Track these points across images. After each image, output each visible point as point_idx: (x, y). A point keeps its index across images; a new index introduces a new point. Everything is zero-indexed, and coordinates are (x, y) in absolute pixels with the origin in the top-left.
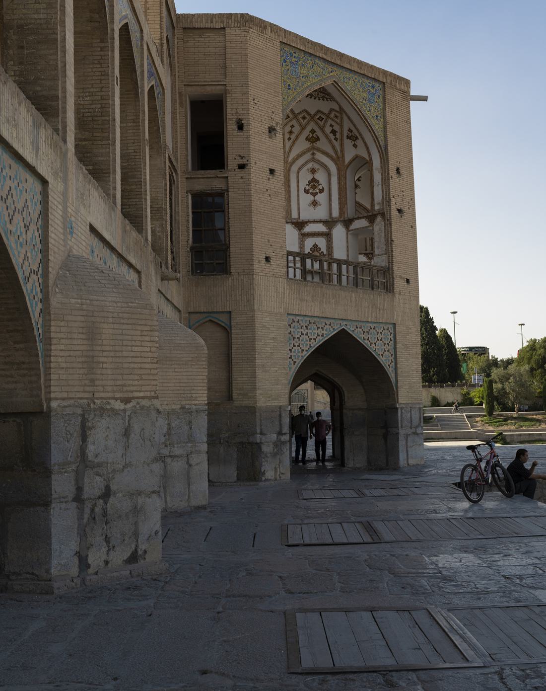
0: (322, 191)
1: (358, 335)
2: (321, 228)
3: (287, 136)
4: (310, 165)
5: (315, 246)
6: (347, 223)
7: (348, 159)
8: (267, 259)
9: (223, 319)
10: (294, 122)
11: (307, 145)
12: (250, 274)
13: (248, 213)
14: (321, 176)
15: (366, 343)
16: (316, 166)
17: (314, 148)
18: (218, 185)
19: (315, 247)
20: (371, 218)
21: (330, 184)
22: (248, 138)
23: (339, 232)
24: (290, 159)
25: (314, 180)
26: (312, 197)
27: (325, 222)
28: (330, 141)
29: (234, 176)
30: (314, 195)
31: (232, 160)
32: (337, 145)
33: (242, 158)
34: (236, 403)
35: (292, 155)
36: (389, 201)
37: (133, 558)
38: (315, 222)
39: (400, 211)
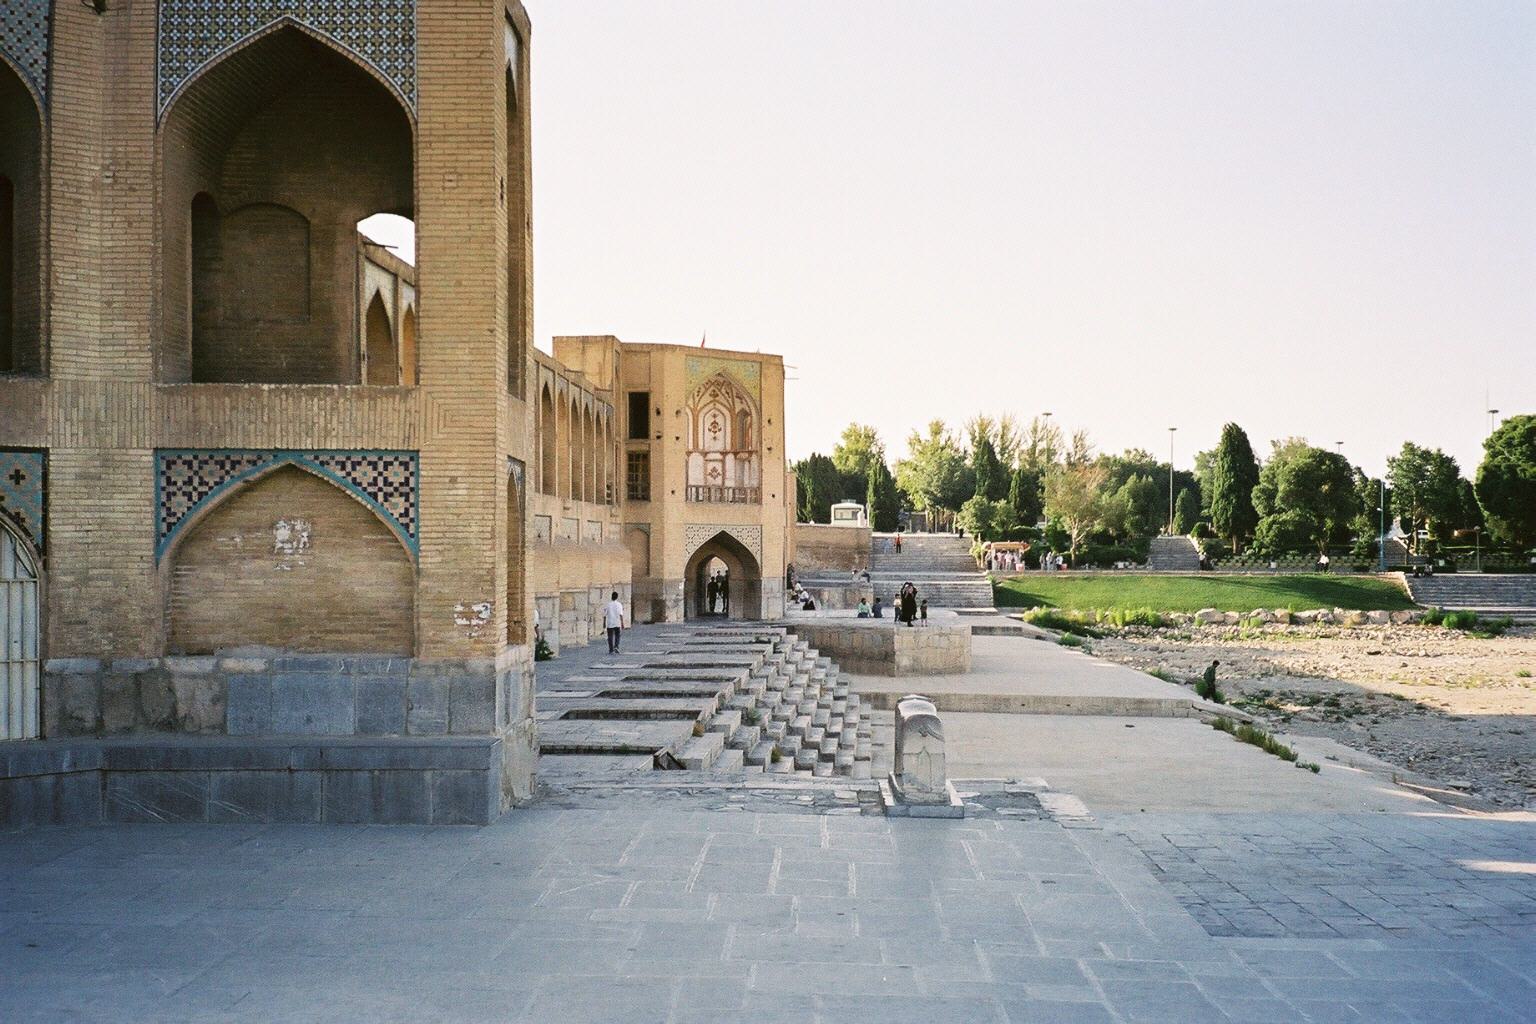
0: (720, 430)
1: (734, 534)
2: (719, 456)
6: (736, 454)
7: (737, 410)
8: (673, 492)
12: (661, 500)
13: (661, 465)
14: (719, 420)
15: (739, 539)
16: (717, 413)
17: (715, 400)
18: (644, 448)
19: (714, 470)
21: (725, 426)
22: (662, 420)
26: (712, 434)
27: (722, 453)
28: (725, 398)
29: (654, 442)
31: (653, 434)
34: (652, 576)
35: (700, 405)
36: (761, 443)
39: (769, 449)
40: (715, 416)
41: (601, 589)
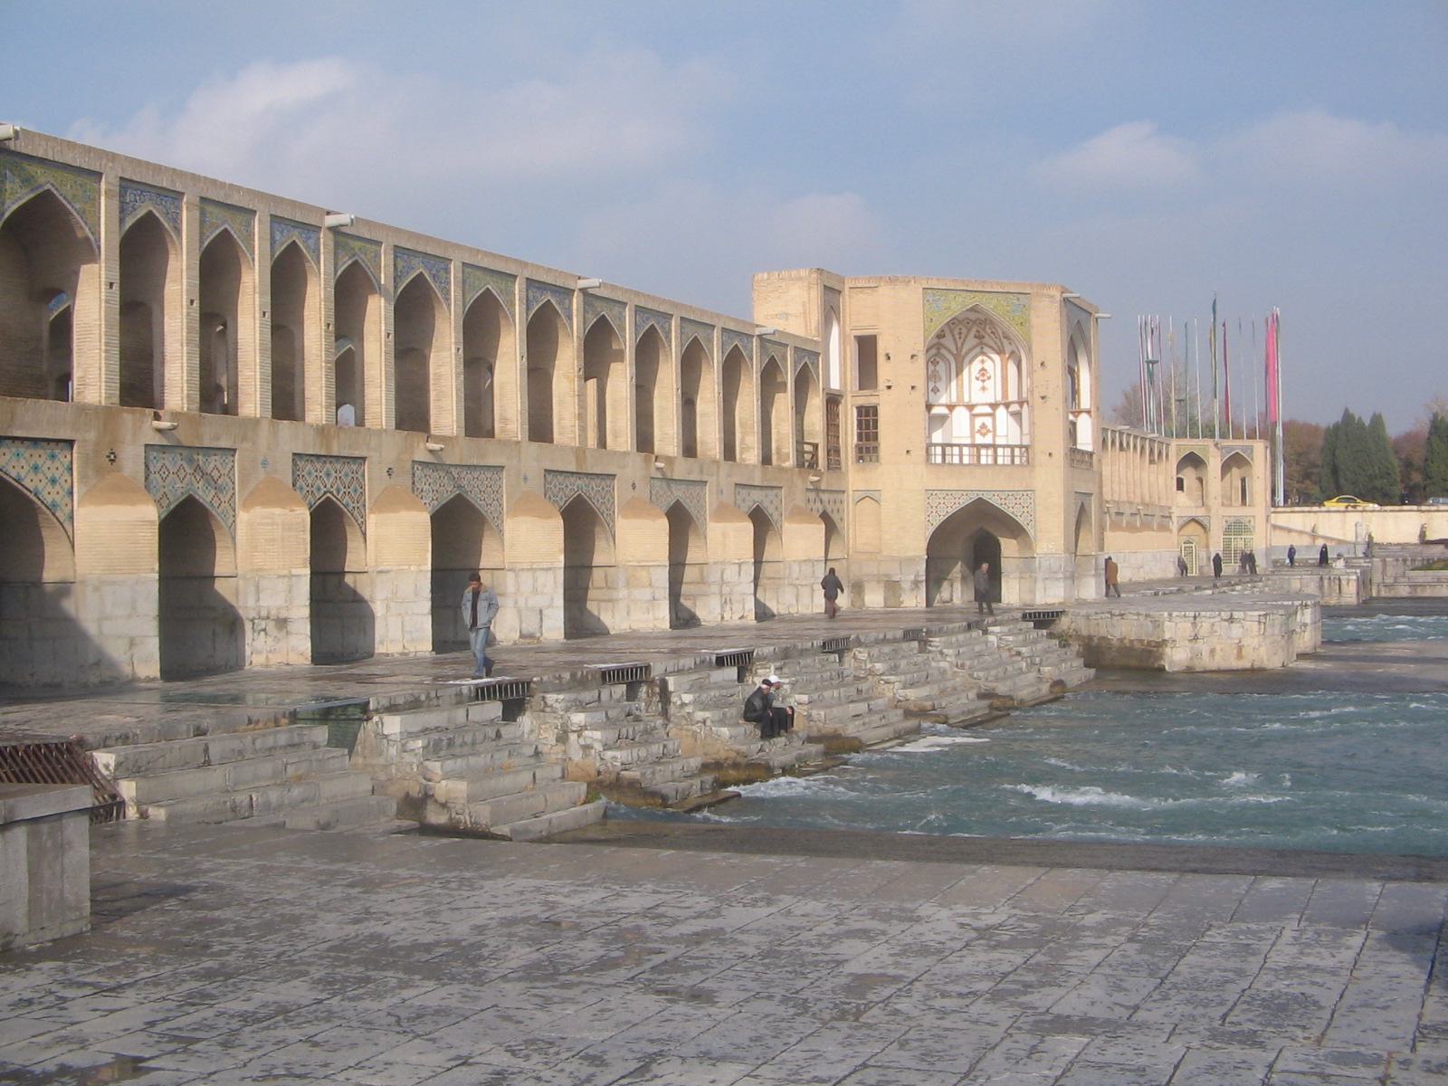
0: (989, 378)
1: (995, 501)
2: (988, 410)
3: (957, 337)
4: (980, 358)
5: (983, 424)
6: (1007, 405)
8: (908, 452)
9: (876, 494)
10: (960, 326)
11: (977, 341)
17: (981, 343)
18: (871, 401)
19: (983, 426)
20: (1021, 404)
23: (1001, 411)
24: (963, 353)
25: (983, 369)
30: (983, 381)
32: (997, 341)
33: (889, 381)
37: (742, 617)
38: (982, 405)
40: (983, 362)
41: (740, 565)
